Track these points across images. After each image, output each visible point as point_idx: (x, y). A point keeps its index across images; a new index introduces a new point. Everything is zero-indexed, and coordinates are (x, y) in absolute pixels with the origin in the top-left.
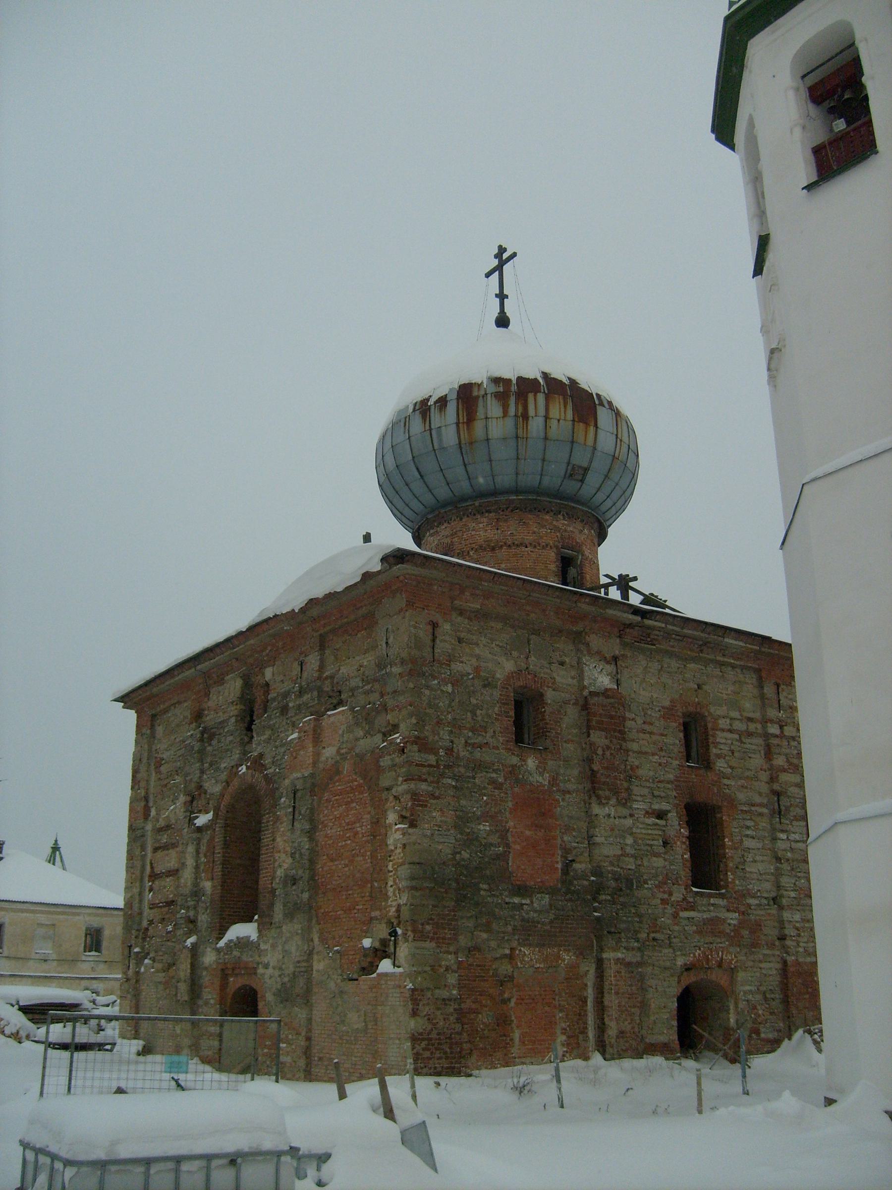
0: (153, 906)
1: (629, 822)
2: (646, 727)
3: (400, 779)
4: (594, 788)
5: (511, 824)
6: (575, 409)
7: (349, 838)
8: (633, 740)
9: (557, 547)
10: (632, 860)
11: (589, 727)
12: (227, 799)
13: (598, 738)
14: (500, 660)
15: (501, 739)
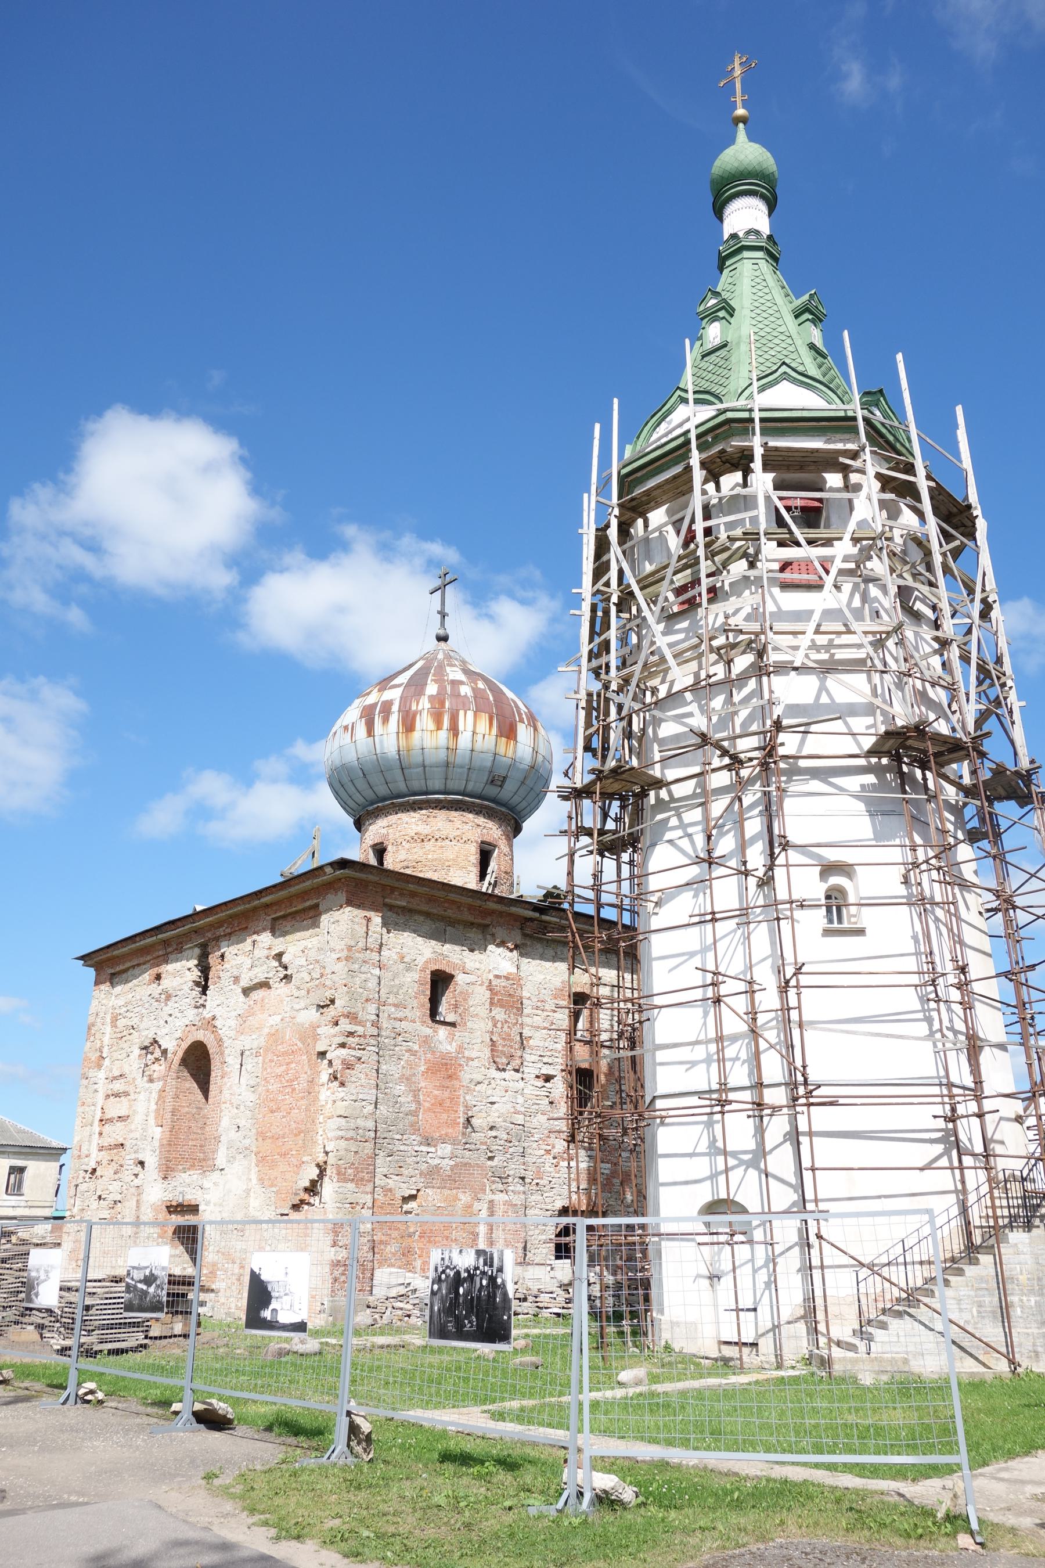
0: (101, 1149)
1: (521, 1084)
2: (539, 1004)
3: (334, 1046)
4: (493, 1056)
5: (423, 1084)
6: (499, 727)
8: (528, 1016)
9: (476, 842)
10: (522, 1116)
11: (492, 1004)
12: (180, 1054)
13: (499, 1014)
14: (420, 947)
15: (418, 1014)
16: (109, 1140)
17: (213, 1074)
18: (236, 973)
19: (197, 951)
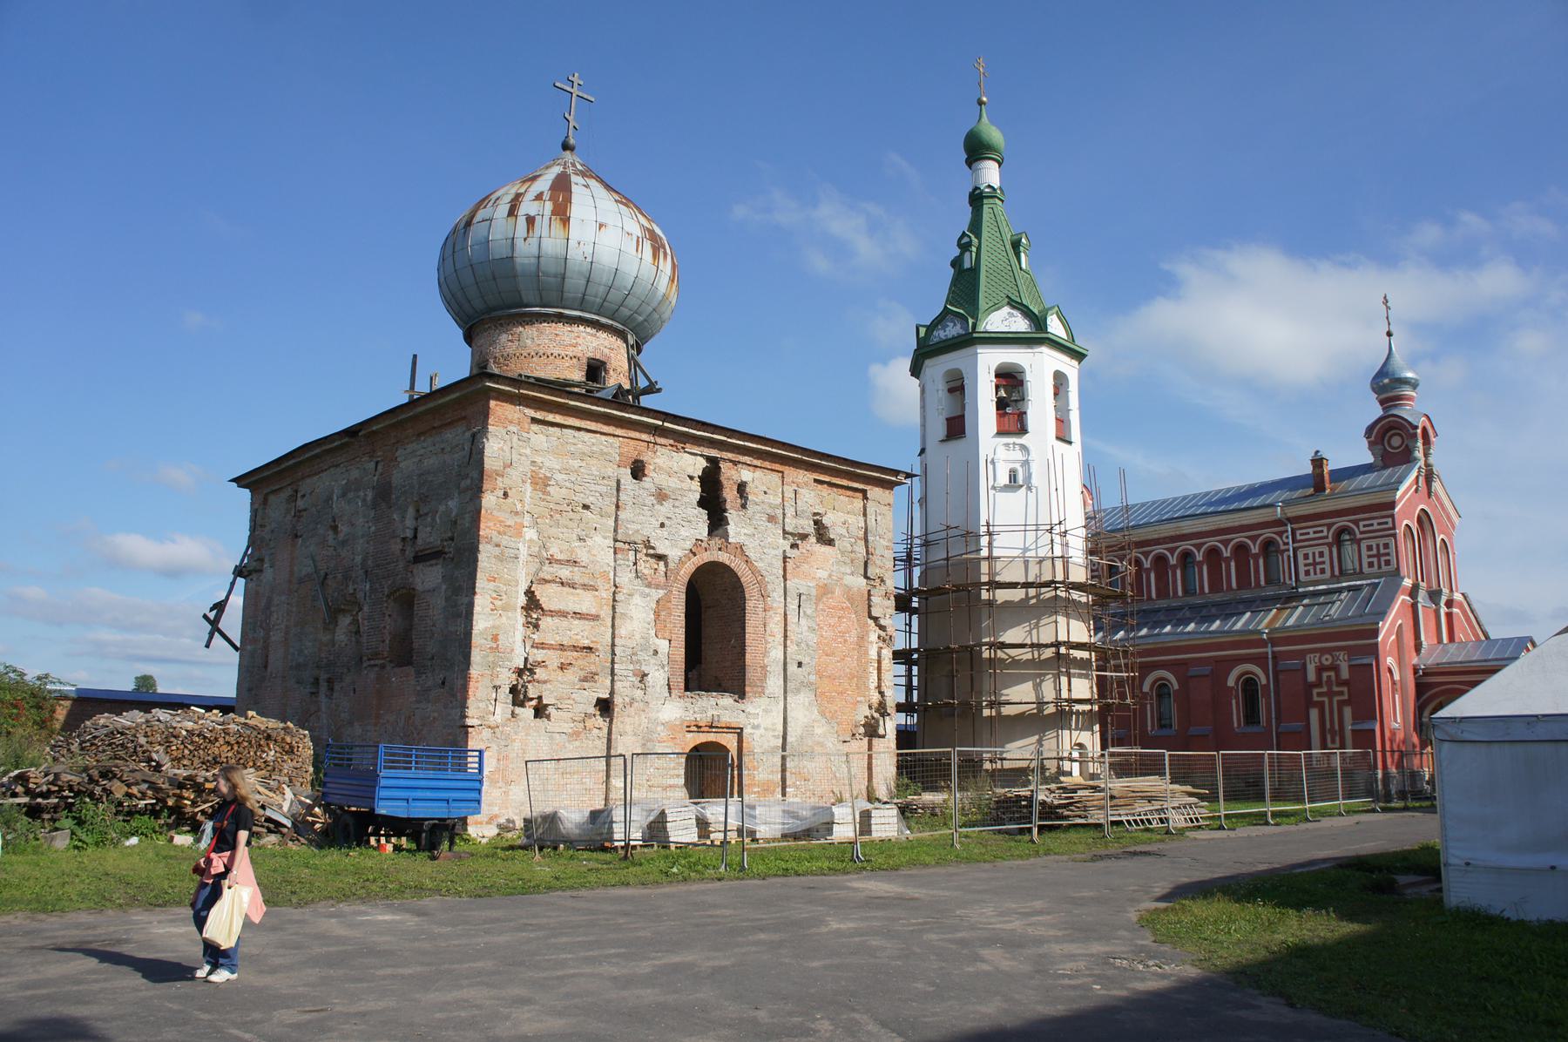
17: (750, 605)
19: (703, 463)
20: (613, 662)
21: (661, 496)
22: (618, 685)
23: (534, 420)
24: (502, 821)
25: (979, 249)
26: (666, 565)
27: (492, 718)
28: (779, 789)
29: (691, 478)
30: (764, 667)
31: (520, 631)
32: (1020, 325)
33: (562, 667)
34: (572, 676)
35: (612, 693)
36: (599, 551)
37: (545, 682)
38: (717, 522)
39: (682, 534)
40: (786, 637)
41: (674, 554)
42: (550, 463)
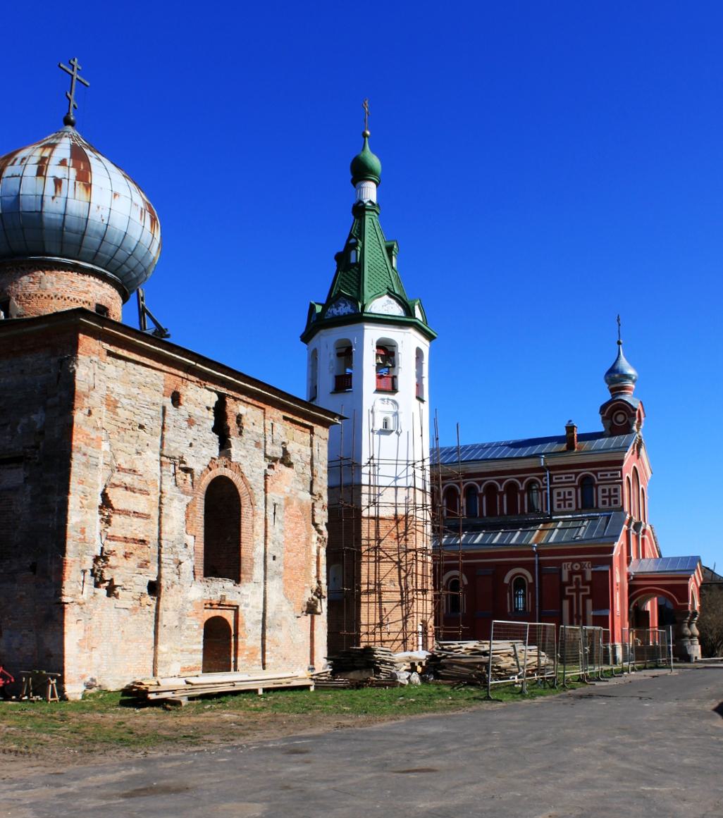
7: (296, 542)
16: (123, 532)
17: (245, 510)
18: (256, 439)
20: (160, 552)
21: (191, 422)
22: (164, 571)
23: (110, 354)
24: (88, 679)
25: (363, 248)
26: (192, 477)
27: (81, 596)
28: (260, 653)
29: (208, 408)
30: (252, 559)
31: (99, 526)
32: (396, 310)
33: (126, 556)
34: (133, 563)
35: (159, 577)
36: (149, 463)
37: (115, 568)
38: (224, 445)
39: (201, 451)
40: (266, 536)
41: (198, 467)
42: (119, 389)
